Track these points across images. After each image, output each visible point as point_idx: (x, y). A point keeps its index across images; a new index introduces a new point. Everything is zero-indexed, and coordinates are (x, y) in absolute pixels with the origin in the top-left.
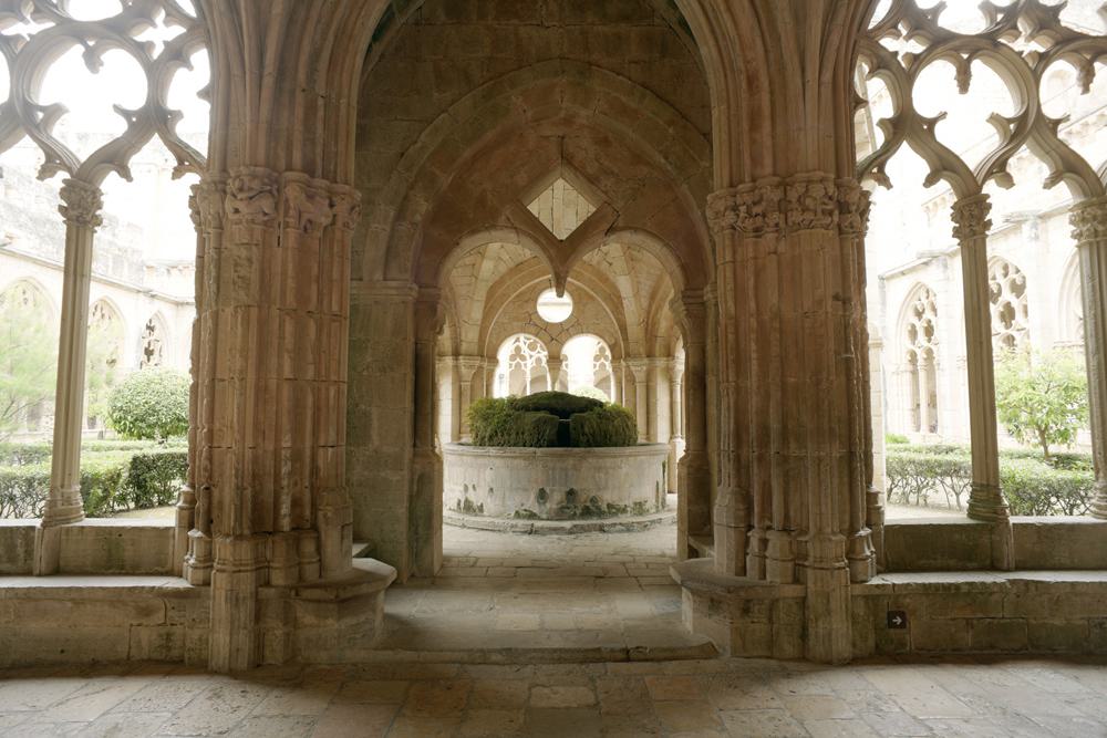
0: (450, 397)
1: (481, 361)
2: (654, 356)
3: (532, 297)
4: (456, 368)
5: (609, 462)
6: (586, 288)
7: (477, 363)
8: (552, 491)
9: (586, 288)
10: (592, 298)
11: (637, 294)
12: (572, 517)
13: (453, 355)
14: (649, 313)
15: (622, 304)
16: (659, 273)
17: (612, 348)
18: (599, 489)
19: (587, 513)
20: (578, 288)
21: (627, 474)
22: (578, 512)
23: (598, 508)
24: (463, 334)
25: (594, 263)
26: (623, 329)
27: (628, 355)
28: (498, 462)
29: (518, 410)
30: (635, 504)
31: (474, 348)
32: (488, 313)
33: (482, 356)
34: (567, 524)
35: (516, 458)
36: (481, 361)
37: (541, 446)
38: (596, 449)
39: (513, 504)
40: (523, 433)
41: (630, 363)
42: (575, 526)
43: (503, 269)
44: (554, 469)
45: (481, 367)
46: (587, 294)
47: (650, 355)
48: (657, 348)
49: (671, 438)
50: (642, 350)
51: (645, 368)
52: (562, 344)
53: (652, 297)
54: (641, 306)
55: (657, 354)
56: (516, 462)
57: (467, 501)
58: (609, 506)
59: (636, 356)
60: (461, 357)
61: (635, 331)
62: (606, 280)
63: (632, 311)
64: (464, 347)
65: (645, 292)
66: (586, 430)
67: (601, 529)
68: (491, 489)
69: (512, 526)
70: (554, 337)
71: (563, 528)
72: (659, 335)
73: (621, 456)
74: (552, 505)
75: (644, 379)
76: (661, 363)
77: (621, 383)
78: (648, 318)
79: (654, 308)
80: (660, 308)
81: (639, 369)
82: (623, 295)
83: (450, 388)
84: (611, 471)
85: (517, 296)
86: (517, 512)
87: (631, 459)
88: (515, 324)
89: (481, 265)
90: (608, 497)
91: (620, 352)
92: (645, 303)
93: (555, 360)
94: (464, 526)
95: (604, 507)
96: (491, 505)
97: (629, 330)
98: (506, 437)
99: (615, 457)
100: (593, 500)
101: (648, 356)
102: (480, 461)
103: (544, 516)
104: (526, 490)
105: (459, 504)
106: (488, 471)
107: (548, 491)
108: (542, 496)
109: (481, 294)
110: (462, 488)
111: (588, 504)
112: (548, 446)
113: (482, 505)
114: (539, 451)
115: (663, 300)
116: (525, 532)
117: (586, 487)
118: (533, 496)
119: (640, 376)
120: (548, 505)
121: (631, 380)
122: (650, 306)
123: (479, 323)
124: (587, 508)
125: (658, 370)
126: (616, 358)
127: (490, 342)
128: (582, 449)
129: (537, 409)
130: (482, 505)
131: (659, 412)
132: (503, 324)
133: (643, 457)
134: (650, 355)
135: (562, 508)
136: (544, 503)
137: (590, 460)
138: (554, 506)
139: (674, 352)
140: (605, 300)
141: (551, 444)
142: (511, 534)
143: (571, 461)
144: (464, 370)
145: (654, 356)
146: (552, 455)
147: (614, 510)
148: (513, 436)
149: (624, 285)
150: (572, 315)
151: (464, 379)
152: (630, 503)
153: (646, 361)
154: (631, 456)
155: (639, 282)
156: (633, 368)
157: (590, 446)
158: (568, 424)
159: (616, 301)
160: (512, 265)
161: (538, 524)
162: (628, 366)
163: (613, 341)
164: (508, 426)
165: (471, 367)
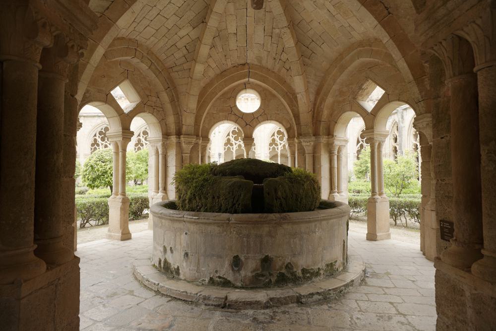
0: (174, 164)
1: (197, 139)
2: (319, 135)
3: (233, 95)
4: (179, 144)
5: (303, 227)
6: (270, 88)
7: (194, 140)
8: (247, 259)
9: (270, 88)
10: (274, 96)
11: (307, 91)
12: (267, 286)
13: (176, 134)
14: (315, 104)
15: (296, 97)
16: (323, 75)
17: (288, 130)
18: (294, 255)
19: (283, 280)
20: (265, 89)
21: (320, 238)
22: (273, 279)
23: (293, 274)
24: (183, 120)
25: (276, 71)
26: (297, 116)
27: (300, 135)
28: (193, 228)
29: (215, 175)
30: (327, 265)
31: (192, 130)
32: (201, 106)
33: (197, 136)
34: (261, 296)
35: (210, 224)
36: (197, 139)
37: (236, 212)
38: (291, 214)
39: (207, 270)
40: (218, 198)
41: (302, 141)
42: (271, 299)
43: (211, 74)
44: (248, 236)
45: (197, 144)
46: (271, 93)
47: (316, 134)
48: (321, 128)
49: (330, 193)
50: (311, 131)
51: (312, 143)
52: (253, 128)
53: (318, 93)
54: (310, 99)
55: (321, 134)
56: (210, 228)
57: (166, 261)
58: (304, 271)
59: (305, 135)
60: (182, 136)
61: (306, 117)
62: (284, 82)
63: (304, 103)
64: (184, 129)
65: (312, 90)
66: (279, 193)
67: (299, 301)
68: (186, 254)
69: (205, 298)
70: (247, 124)
71: (258, 303)
72: (323, 120)
73: (316, 221)
74: (247, 272)
75: (311, 151)
76: (324, 140)
77: (294, 154)
78: (314, 108)
79: (319, 101)
80: (323, 100)
81: (308, 144)
82: (297, 91)
83: (175, 158)
84: (305, 236)
85: (223, 95)
86: (211, 279)
87: (324, 223)
88: (221, 114)
89: (194, 67)
90: (303, 262)
91: (294, 133)
92: (312, 98)
93: (249, 140)
94: (158, 292)
95: (299, 273)
96: (186, 270)
97: (301, 116)
98: (203, 200)
99: (310, 222)
100: (289, 267)
101: (314, 135)
102: (177, 225)
103: (239, 284)
104: (219, 257)
105: (160, 263)
106: (183, 236)
107: (243, 258)
108: (237, 263)
109: (195, 91)
110: (162, 249)
111: (283, 271)
112: (243, 212)
113: (178, 267)
114: (234, 217)
115: (326, 95)
116: (218, 306)
117: (281, 254)
118: (227, 264)
119: (308, 149)
120: (243, 273)
121: (302, 152)
122: (316, 100)
123: (195, 111)
124: (282, 275)
125: (322, 144)
126: (290, 138)
127: (203, 127)
128: (277, 215)
129: (233, 174)
130: (178, 267)
131: (322, 175)
132: (213, 114)
133: (335, 220)
134: (316, 134)
135: (258, 275)
136: (239, 270)
137: (286, 226)
138: (249, 274)
139: (333, 132)
140: (283, 97)
141: (245, 211)
142: (203, 307)
143: (266, 229)
144: (184, 145)
145: (319, 135)
146: (247, 222)
147: (309, 274)
148: (210, 199)
149: (298, 84)
150: (260, 107)
151: (184, 152)
152: (322, 265)
153: (313, 138)
154: (324, 220)
155: (308, 82)
156: (304, 144)
157: (284, 212)
158: (262, 188)
159: (292, 98)
160: (218, 72)
161: (235, 295)
162: (300, 143)
163: (289, 126)
164: (205, 190)
165: (190, 143)
